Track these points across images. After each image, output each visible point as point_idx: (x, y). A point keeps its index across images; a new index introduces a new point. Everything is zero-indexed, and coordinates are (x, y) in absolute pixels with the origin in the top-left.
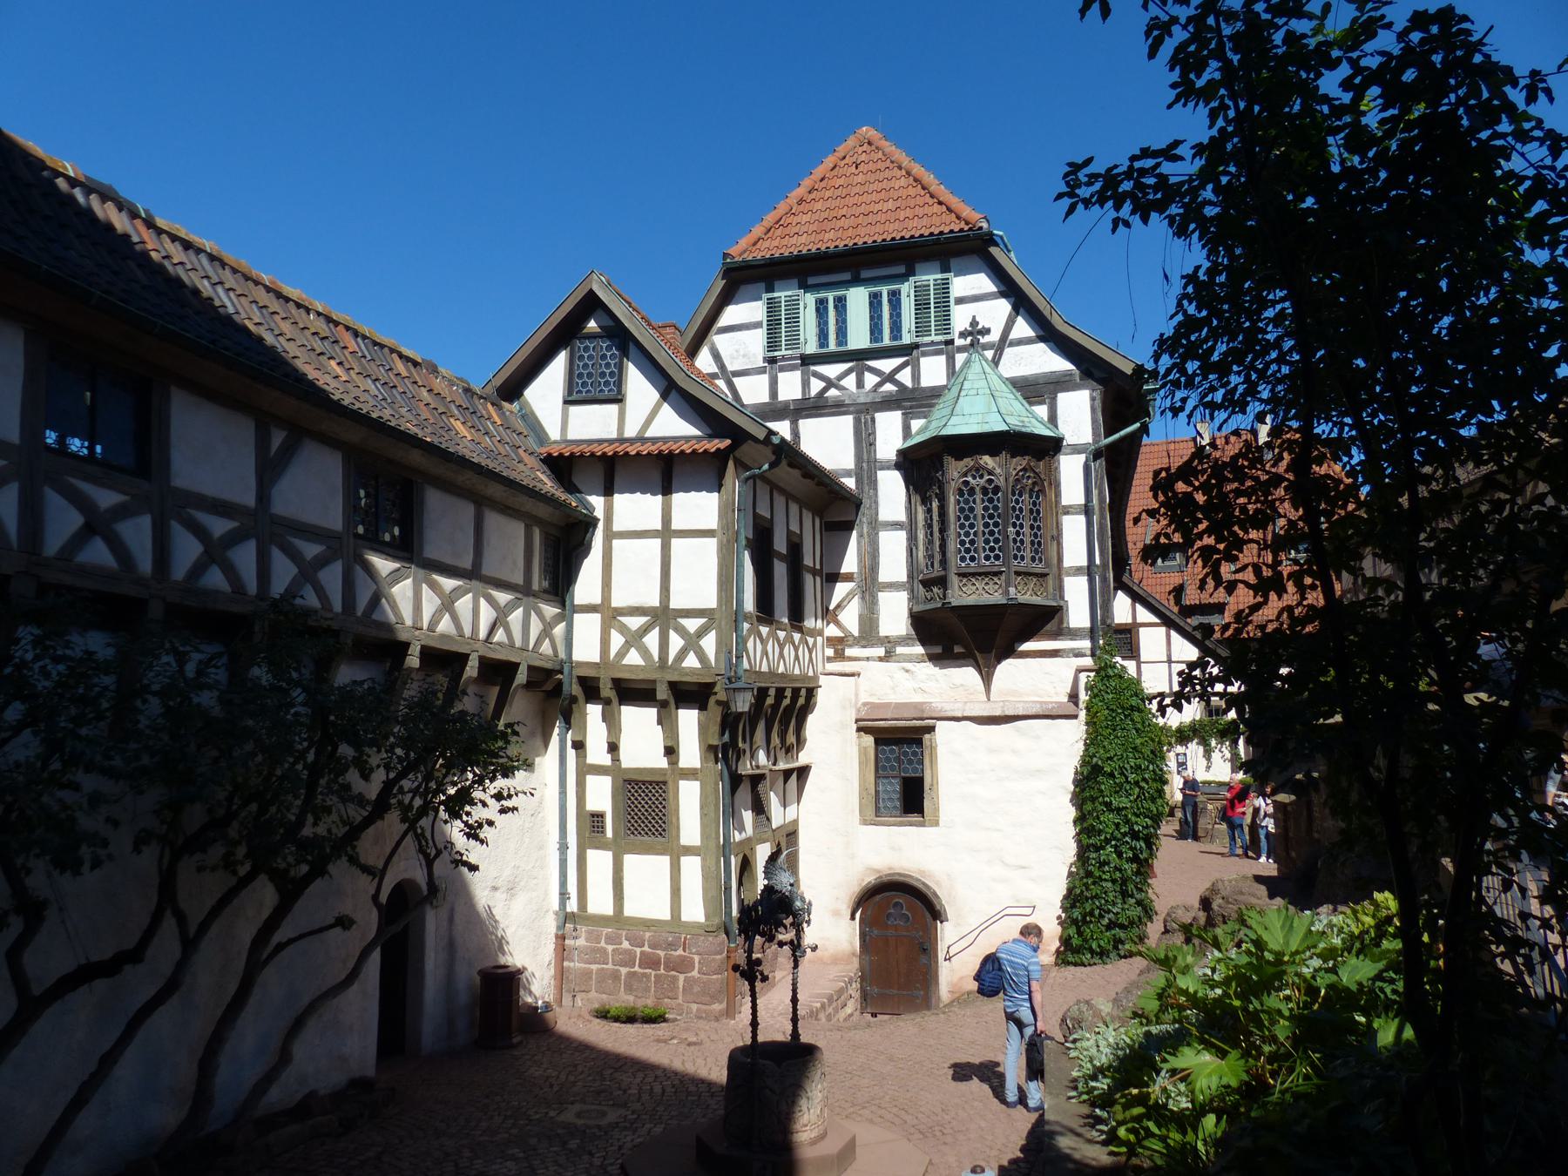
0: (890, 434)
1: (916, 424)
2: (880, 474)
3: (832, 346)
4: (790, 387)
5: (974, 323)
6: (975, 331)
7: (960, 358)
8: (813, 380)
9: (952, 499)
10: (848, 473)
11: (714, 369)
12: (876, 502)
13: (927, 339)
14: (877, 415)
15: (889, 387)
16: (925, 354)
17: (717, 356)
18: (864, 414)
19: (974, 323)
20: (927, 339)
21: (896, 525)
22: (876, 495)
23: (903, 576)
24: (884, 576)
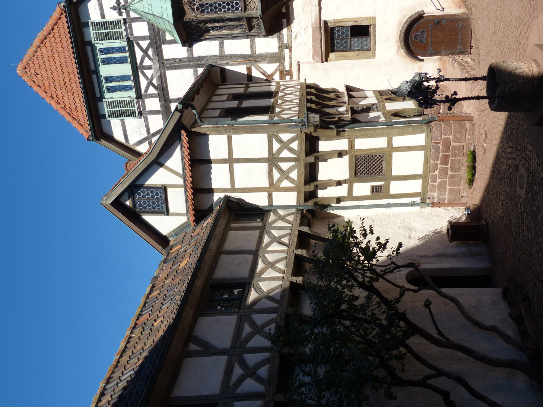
0: (174, 50)
1: (169, 37)
2: (195, 55)
7: (133, 15)
9: (206, 16)
10: (196, 72)
11: (147, 144)
12: (210, 57)
15: (150, 52)
16: (132, 34)
17: (140, 142)
18: (165, 65)
19: (114, 8)
21: (221, 46)
22: (206, 57)
23: (247, 41)
24: (247, 51)
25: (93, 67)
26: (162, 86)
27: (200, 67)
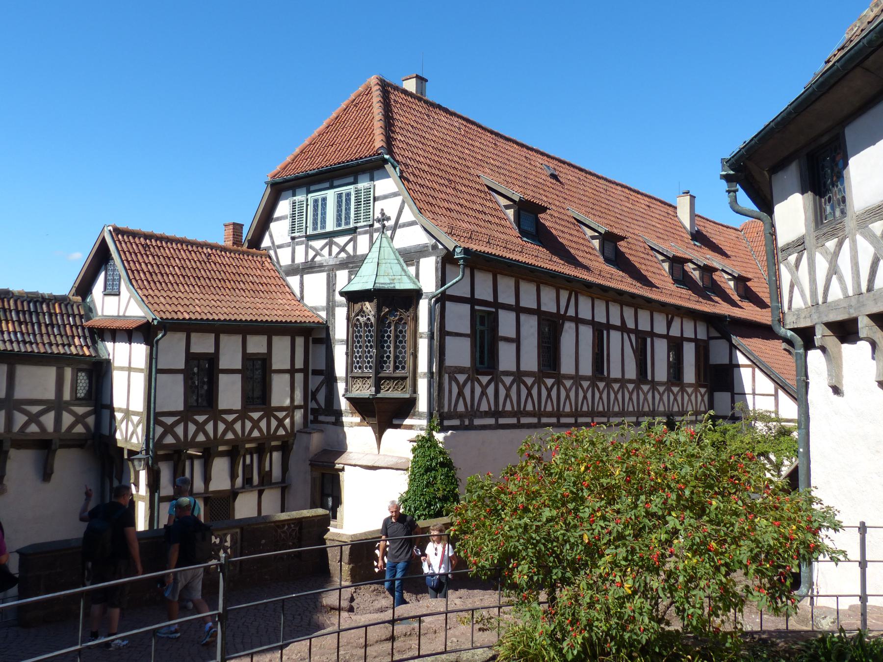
3: (319, 231)
10: (322, 309)
15: (343, 255)
16: (360, 234)
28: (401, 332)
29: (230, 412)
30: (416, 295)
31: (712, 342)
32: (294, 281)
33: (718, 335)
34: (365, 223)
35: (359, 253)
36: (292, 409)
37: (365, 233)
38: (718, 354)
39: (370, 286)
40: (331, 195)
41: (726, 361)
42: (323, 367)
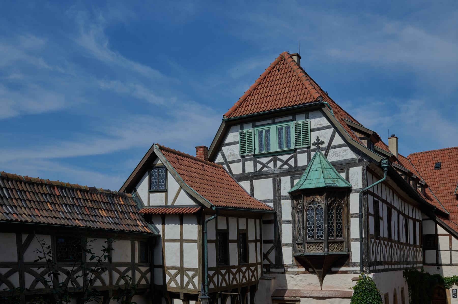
1: (296, 181)
2: (283, 201)
3: (265, 151)
4: (250, 168)
5: (318, 139)
6: (319, 142)
7: (313, 154)
8: (258, 164)
10: (270, 201)
11: (222, 161)
12: (281, 213)
13: (299, 147)
14: (281, 178)
17: (223, 156)
19: (318, 139)
20: (299, 147)
21: (288, 222)
24: (284, 241)
25: (277, 120)
26: (262, 175)
27: (274, 204)
28: (339, 214)
29: (234, 267)
30: (348, 190)
31: (424, 222)
32: (245, 185)
33: (428, 218)
34: (304, 146)
35: (300, 164)
36: (255, 265)
37: (304, 152)
38: (429, 228)
39: (323, 185)
40: (274, 129)
41: (434, 233)
42: (273, 238)
